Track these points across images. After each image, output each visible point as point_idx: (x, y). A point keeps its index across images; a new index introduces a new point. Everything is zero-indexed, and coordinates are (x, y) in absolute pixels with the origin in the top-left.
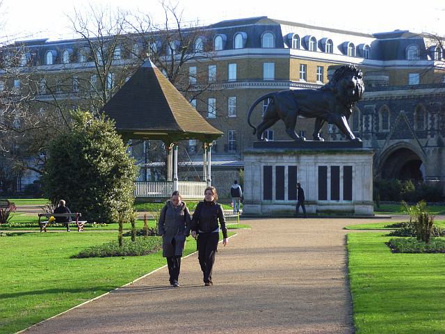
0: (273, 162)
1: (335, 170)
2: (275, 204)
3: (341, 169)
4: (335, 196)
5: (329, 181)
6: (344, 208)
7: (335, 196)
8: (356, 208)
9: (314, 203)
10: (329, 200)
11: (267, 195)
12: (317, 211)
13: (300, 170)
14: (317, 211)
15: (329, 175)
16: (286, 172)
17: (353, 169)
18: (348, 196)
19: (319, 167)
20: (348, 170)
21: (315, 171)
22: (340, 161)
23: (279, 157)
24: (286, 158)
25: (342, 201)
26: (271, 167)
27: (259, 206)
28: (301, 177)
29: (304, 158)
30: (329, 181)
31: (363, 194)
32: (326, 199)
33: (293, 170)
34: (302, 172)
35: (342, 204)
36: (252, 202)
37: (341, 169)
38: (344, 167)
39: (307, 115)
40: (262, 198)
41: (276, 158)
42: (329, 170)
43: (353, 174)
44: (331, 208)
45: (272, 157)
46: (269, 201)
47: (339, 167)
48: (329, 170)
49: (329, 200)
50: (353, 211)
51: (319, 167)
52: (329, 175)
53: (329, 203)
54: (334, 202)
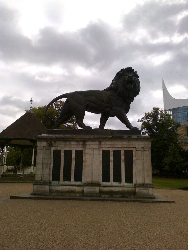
0: (62, 147)
1: (117, 154)
2: (62, 185)
3: (123, 152)
4: (117, 179)
5: (111, 164)
6: (126, 189)
7: (117, 179)
8: (137, 190)
10: (112, 182)
11: (56, 177)
13: (86, 154)
15: (111, 158)
16: (73, 155)
17: (134, 153)
18: (129, 178)
20: (129, 154)
21: (99, 154)
23: (68, 143)
24: (74, 143)
25: (123, 183)
27: (47, 187)
28: (86, 158)
29: (90, 144)
30: (111, 164)
31: (144, 178)
32: (108, 181)
33: (80, 154)
34: (87, 155)
35: (124, 185)
36: (42, 183)
37: (123, 152)
38: (125, 151)
40: (51, 179)
41: (64, 143)
42: (112, 154)
43: (134, 158)
45: (61, 142)
46: (57, 182)
47: (120, 152)
48: (112, 154)
49: (112, 182)
50: (134, 193)
52: (111, 158)
53: (112, 185)
54: (117, 184)
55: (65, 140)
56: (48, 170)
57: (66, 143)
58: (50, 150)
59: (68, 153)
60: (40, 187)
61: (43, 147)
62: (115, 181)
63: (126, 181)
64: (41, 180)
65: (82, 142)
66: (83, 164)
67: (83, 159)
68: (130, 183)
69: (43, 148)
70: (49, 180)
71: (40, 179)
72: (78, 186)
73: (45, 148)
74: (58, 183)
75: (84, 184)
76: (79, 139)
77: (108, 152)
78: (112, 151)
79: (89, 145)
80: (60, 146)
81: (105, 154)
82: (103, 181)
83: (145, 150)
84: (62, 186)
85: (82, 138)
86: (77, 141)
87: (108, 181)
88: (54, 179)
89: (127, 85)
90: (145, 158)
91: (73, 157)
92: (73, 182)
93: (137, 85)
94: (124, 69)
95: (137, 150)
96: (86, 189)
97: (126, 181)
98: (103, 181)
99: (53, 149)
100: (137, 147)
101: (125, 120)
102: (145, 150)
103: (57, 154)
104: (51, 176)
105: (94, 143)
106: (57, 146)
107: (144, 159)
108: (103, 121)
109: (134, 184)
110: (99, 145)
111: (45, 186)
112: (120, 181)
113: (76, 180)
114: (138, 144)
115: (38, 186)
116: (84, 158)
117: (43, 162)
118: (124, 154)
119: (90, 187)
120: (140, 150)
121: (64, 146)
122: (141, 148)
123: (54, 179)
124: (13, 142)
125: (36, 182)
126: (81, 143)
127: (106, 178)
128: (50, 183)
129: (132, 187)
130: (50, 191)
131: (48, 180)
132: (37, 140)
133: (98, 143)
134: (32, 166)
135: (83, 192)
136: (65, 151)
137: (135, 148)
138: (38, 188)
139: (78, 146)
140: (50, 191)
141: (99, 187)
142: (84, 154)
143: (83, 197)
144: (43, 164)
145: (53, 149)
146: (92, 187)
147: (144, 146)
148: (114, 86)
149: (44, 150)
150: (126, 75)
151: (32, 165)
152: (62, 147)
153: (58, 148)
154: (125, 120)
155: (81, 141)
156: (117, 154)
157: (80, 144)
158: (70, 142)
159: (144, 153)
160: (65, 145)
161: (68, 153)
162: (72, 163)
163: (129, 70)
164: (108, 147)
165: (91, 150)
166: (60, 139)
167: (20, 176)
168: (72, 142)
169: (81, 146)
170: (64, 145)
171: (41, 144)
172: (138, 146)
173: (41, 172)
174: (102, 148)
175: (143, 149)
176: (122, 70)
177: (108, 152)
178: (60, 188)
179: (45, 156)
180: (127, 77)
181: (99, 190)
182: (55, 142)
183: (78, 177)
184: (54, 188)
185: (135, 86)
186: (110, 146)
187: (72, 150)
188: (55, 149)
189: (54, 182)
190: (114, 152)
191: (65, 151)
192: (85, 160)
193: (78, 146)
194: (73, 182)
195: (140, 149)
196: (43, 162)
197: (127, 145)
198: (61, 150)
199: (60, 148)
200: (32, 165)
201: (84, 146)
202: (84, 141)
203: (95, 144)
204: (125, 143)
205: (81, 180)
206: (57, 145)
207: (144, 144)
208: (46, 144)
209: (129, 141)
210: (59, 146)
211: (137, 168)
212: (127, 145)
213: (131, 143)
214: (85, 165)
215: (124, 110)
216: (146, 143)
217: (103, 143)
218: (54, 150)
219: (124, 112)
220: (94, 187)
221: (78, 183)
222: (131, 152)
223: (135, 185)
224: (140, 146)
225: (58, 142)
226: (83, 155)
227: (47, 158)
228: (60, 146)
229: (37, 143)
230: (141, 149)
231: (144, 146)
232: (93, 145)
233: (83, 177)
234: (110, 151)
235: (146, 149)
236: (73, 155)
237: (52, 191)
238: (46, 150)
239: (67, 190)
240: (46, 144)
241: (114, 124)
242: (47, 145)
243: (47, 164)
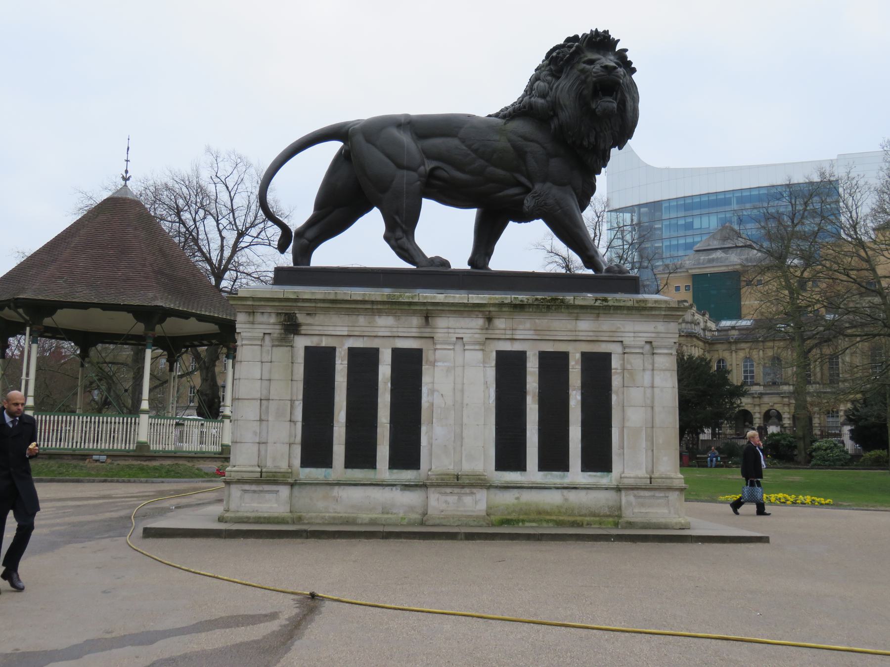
1: (554, 365)
9: (479, 483)
11: (315, 451)
15: (532, 383)
16: (385, 371)
17: (615, 363)
19: (500, 355)
20: (598, 368)
22: (573, 334)
23: (362, 320)
24: (385, 323)
25: (576, 474)
26: (330, 352)
32: (520, 466)
33: (409, 366)
38: (584, 355)
39: (453, 196)
40: (297, 461)
42: (532, 366)
43: (616, 381)
47: (565, 356)
48: (532, 366)
52: (532, 383)
54: (554, 478)
58: (292, 346)
61: (262, 335)
62: (545, 465)
72: (407, 487)
77: (520, 358)
78: (535, 354)
81: (509, 368)
87: (520, 466)
88: (308, 461)
89: (585, 98)
93: (629, 104)
94: (576, 38)
95: (627, 350)
100: (627, 341)
103: (319, 362)
104: (297, 451)
108: (486, 237)
110: (484, 331)
112: (563, 466)
113: (394, 464)
114: (631, 330)
116: (426, 379)
118: (579, 367)
120: (640, 351)
121: (346, 333)
123: (308, 461)
124: (63, 318)
127: (509, 455)
134: (144, 419)
136: (353, 353)
137: (619, 344)
145: (301, 343)
147: (653, 335)
148: (541, 101)
150: (591, 62)
151: (145, 412)
153: (324, 338)
156: (554, 365)
161: (363, 361)
162: (379, 400)
163: (601, 42)
165: (454, 349)
167: (95, 457)
170: (346, 329)
172: (632, 335)
174: (496, 342)
176: (568, 40)
177: (520, 358)
179: (270, 372)
180: (597, 68)
183: (406, 454)
185: (622, 104)
186: (529, 337)
187: (377, 350)
188: (309, 344)
189: (307, 470)
190: (544, 357)
191: (353, 353)
197: (591, 334)
198: (333, 349)
200: (145, 412)
202: (428, 313)
204: (585, 326)
209: (598, 317)
212: (591, 334)
213: (607, 324)
215: (575, 197)
216: (661, 327)
218: (307, 348)
219: (574, 204)
221: (407, 475)
222: (607, 357)
224: (641, 335)
228: (331, 331)
230: (642, 348)
231: (653, 335)
236: (385, 371)
238: (273, 346)
241: (528, 246)
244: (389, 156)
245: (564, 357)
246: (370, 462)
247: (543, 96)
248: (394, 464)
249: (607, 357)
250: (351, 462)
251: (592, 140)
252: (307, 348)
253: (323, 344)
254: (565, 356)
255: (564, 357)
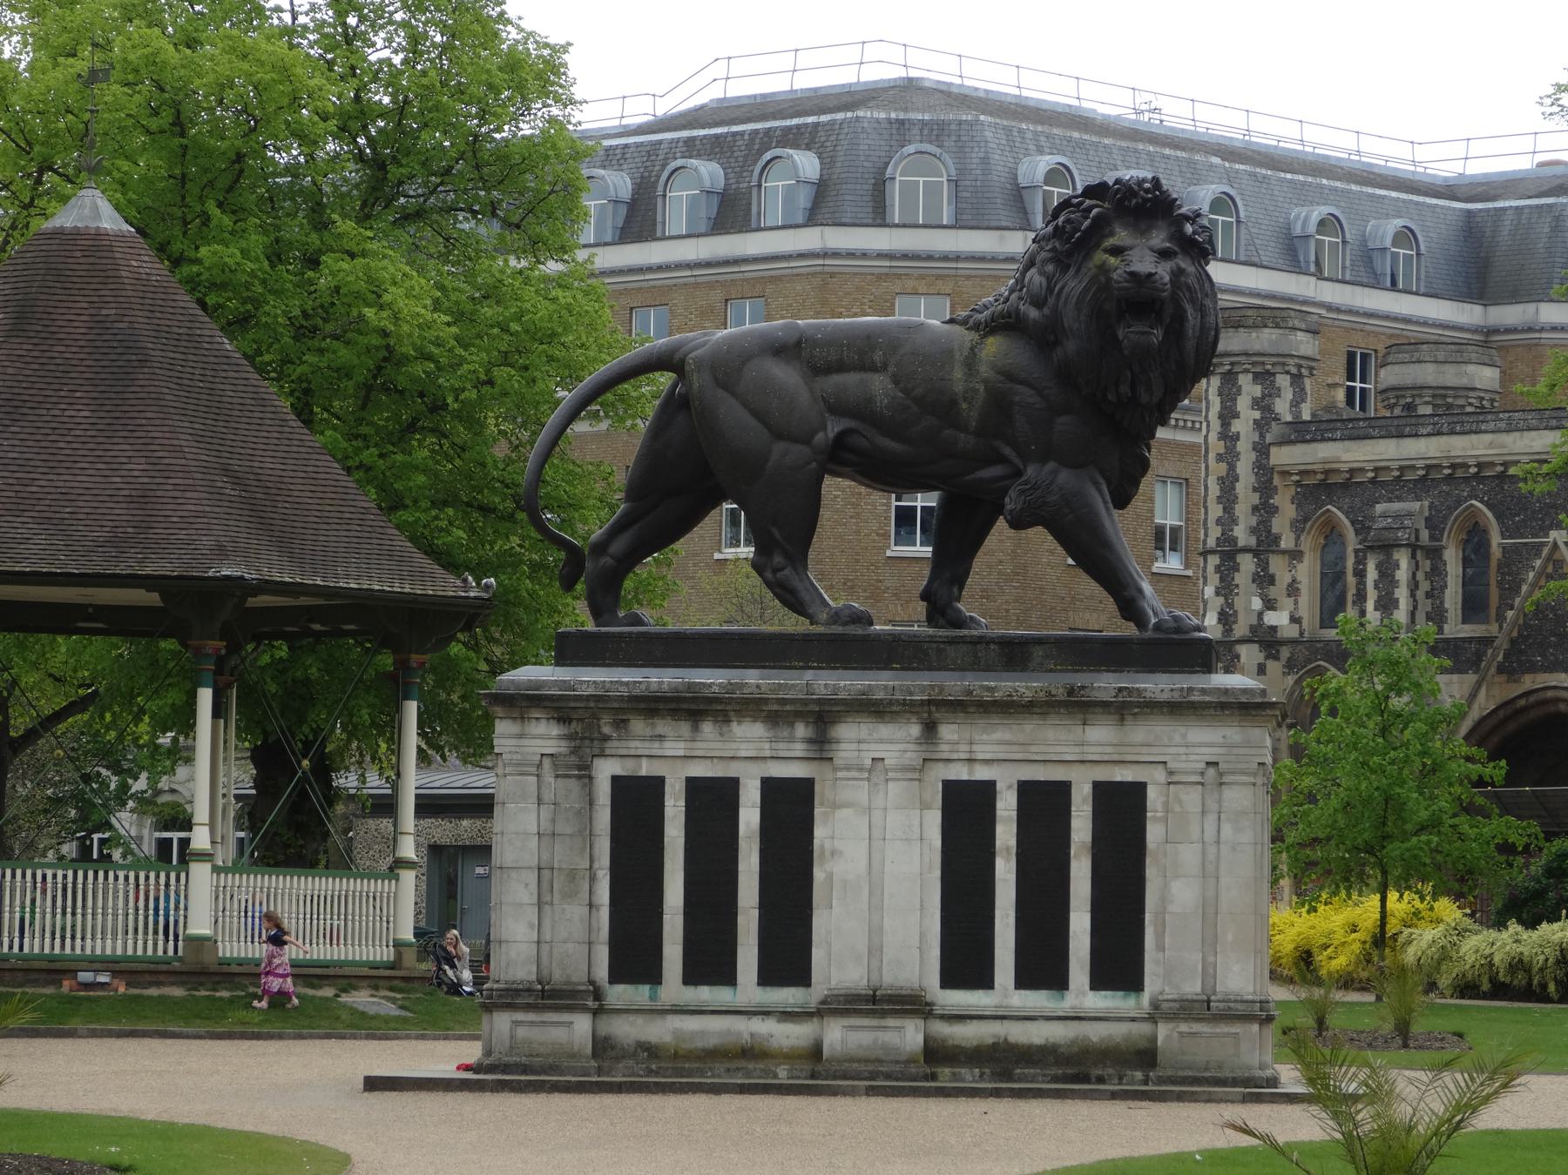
0: (675, 758)
1: (1044, 804)
4: (1042, 966)
5: (1005, 872)
9: (911, 1004)
10: (1005, 991)
11: (634, 955)
12: (936, 1053)
13: (835, 806)
14: (936, 1053)
15: (1006, 834)
16: (749, 817)
18: (1119, 965)
19: (947, 784)
20: (1122, 809)
23: (707, 728)
24: (749, 735)
25: (1081, 994)
27: (582, 1025)
29: (857, 740)
30: (1005, 872)
32: (982, 978)
33: (791, 808)
36: (548, 996)
38: (1097, 786)
40: (602, 972)
41: (685, 728)
42: (1007, 805)
43: (1154, 834)
44: (1019, 1033)
46: (645, 989)
47: (1064, 788)
48: (1007, 805)
49: (1005, 991)
51: (947, 784)
52: (1006, 834)
53: (1005, 1007)
54: (1037, 1000)
55: (692, 709)
56: (575, 911)
57: (696, 728)
58: (590, 778)
59: (712, 801)
60: (532, 1023)
62: (1026, 978)
63: (1099, 981)
64: (534, 977)
65: (807, 723)
66: (818, 874)
67: (816, 841)
68: (1120, 993)
69: (540, 765)
70: (592, 982)
71: (530, 972)
72: (787, 1016)
73: (555, 766)
74: (653, 998)
75: (823, 1002)
76: (788, 708)
78: (1010, 787)
79: (854, 746)
80: (654, 752)
81: (966, 810)
82: (948, 981)
83: (1225, 779)
84: (677, 1012)
85: (805, 702)
86: (775, 713)
87: (982, 978)
88: (618, 974)
90: (1227, 830)
91: (748, 824)
92: (748, 985)
95: (1175, 778)
96: (837, 1036)
97: (1099, 981)
98: (948, 981)
99: (605, 770)
101: (1097, 559)
102: (1225, 779)
103: (637, 802)
104: (602, 955)
105: (885, 730)
106: (632, 752)
107: (1218, 842)
109: (1146, 998)
110: (924, 747)
111: (566, 1017)
112: (1058, 981)
113: (768, 977)
115: (520, 1016)
116: (819, 832)
117: (545, 856)
119: (866, 1022)
121: (681, 753)
122: (1203, 765)
125: (507, 990)
126: (801, 730)
127: (965, 960)
128: (598, 994)
129: (1133, 1020)
130: (603, 1047)
131: (579, 976)
132: (498, 710)
133: (915, 730)
135: (816, 1052)
136: (695, 787)
137: (1160, 767)
138: (521, 1032)
139: (783, 749)
140: (603, 1047)
141: (920, 1023)
142: (822, 804)
143: (817, 1075)
144: (546, 873)
145: (605, 770)
146: (874, 1022)
148: (1033, 313)
149: (549, 778)
152: (675, 758)
153: (644, 761)
154: (1097, 559)
155: (800, 715)
157: (792, 740)
158: (728, 721)
159: (1220, 802)
160: (689, 745)
161: (712, 801)
164: (988, 756)
165: (868, 779)
166: (653, 706)
168: (739, 722)
169: (799, 749)
170: (682, 745)
171: (521, 736)
173: (531, 926)
175: (1215, 773)
178: (661, 1031)
179: (553, 821)
181: (920, 1039)
182: (621, 724)
183: (787, 958)
184: (627, 1030)
188: (619, 771)
189: (620, 988)
191: (695, 787)
192: (827, 845)
193: (781, 754)
194: (748, 985)
195: (1194, 773)
196: (545, 856)
198: (660, 781)
199: (655, 762)
201: (821, 746)
202: (822, 718)
203: (892, 742)
204: (1100, 734)
205: (801, 977)
206: (636, 746)
207: (1221, 740)
208: (560, 737)
209: (1122, 719)
210: (647, 752)
211: (1172, 890)
213: (1141, 732)
214: (830, 877)
217: (947, 732)
218: (615, 779)
220: (891, 1022)
221: (787, 996)
222: (1139, 789)
223: (1155, 1005)
224: (1197, 750)
225: (638, 726)
226: (818, 811)
227: (568, 830)
229: (497, 730)
232: (881, 747)
233: (817, 955)
234: (999, 786)
235: (1233, 773)
236: (749, 817)
237: (612, 1048)
238: (557, 776)
239: (711, 1042)
240: (560, 737)
242: (564, 743)
243: (572, 875)
244: (755, 414)
245: (1062, 790)
246: (725, 975)
247: (1038, 303)
248: (768, 977)
249: (1139, 789)
250: (694, 974)
251: (1125, 389)
252: (615, 779)
253: (643, 772)
254: (1064, 788)
255: (1062, 790)
